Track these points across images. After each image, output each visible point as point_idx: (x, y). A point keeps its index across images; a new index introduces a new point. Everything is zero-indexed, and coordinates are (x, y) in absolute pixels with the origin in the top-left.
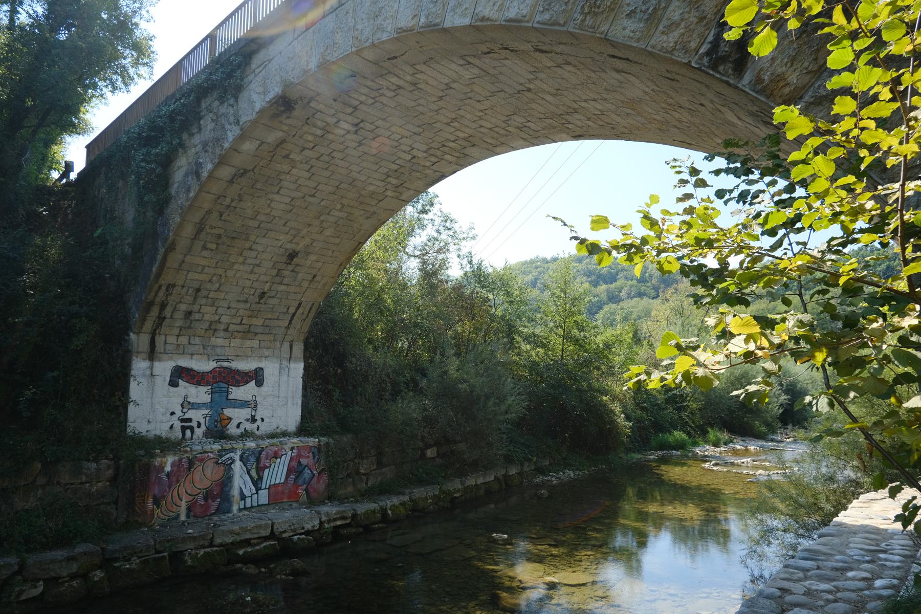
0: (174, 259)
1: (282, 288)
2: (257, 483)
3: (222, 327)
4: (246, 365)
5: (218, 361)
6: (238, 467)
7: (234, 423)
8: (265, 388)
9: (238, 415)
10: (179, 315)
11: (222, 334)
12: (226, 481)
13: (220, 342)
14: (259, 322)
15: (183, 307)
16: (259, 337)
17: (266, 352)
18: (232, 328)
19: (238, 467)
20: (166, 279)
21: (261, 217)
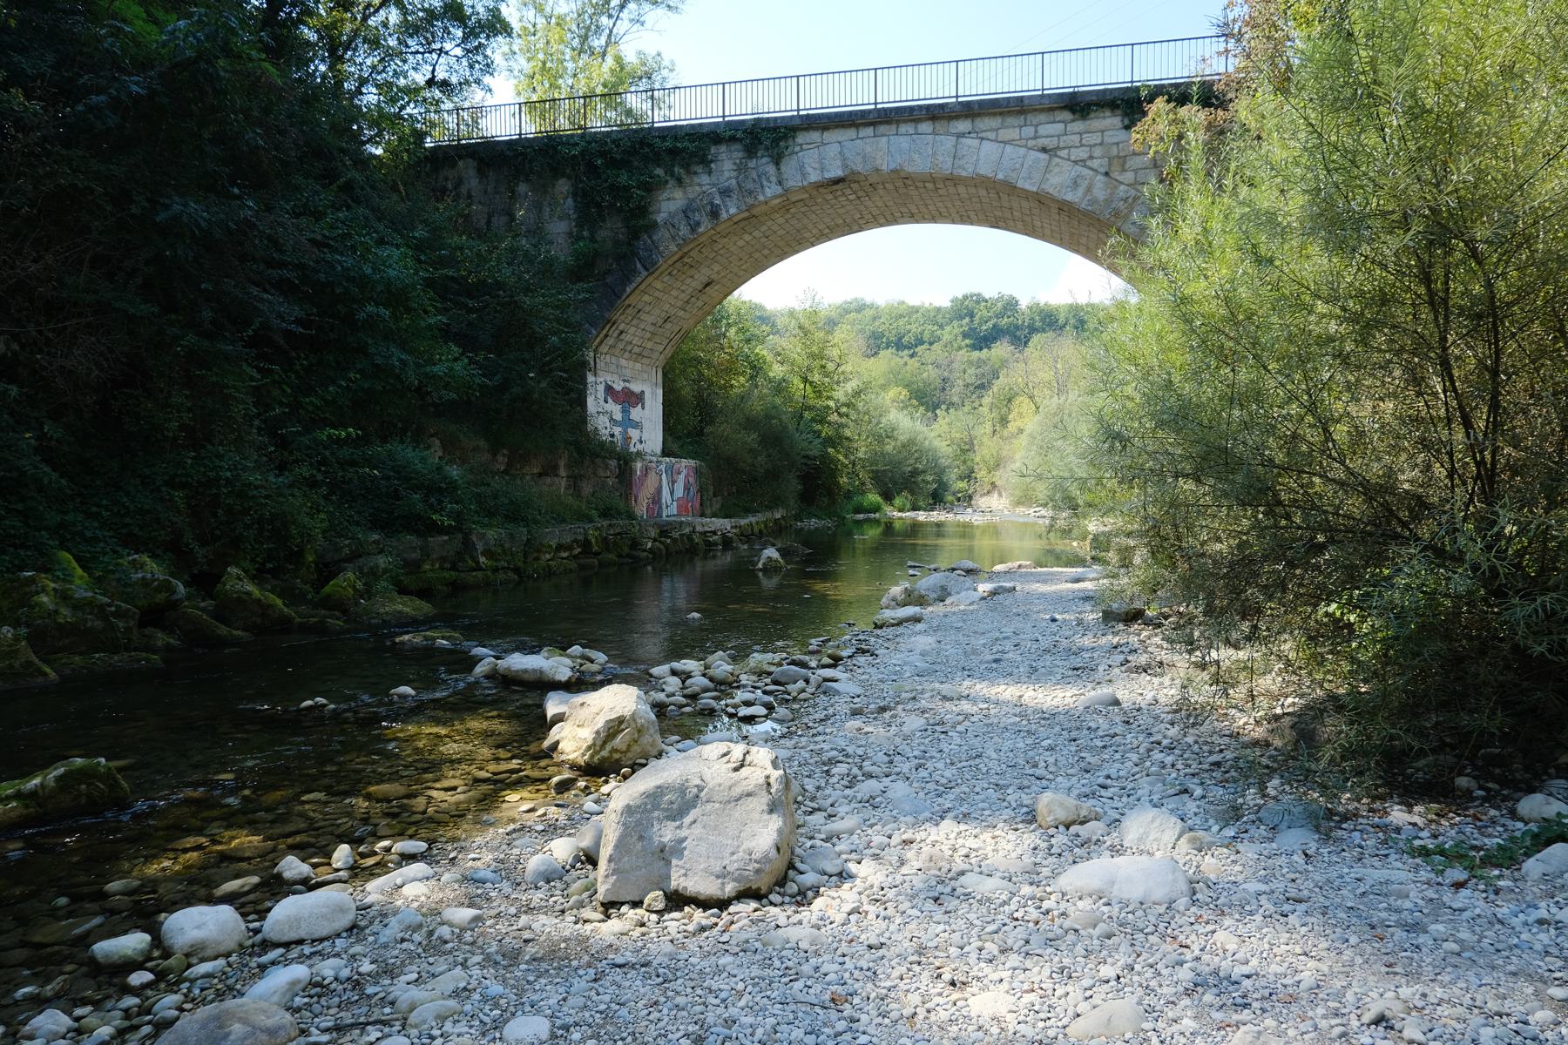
0: (650, 279)
1: (681, 313)
2: (672, 493)
3: (629, 348)
4: (636, 387)
5: (624, 381)
6: (664, 475)
7: (633, 442)
8: (646, 411)
9: (634, 434)
10: (615, 335)
11: (627, 355)
12: (659, 491)
13: (623, 362)
14: (650, 345)
15: (622, 327)
16: (645, 361)
17: (645, 376)
18: (636, 350)
19: (664, 475)
20: (627, 302)
21: (722, 252)
